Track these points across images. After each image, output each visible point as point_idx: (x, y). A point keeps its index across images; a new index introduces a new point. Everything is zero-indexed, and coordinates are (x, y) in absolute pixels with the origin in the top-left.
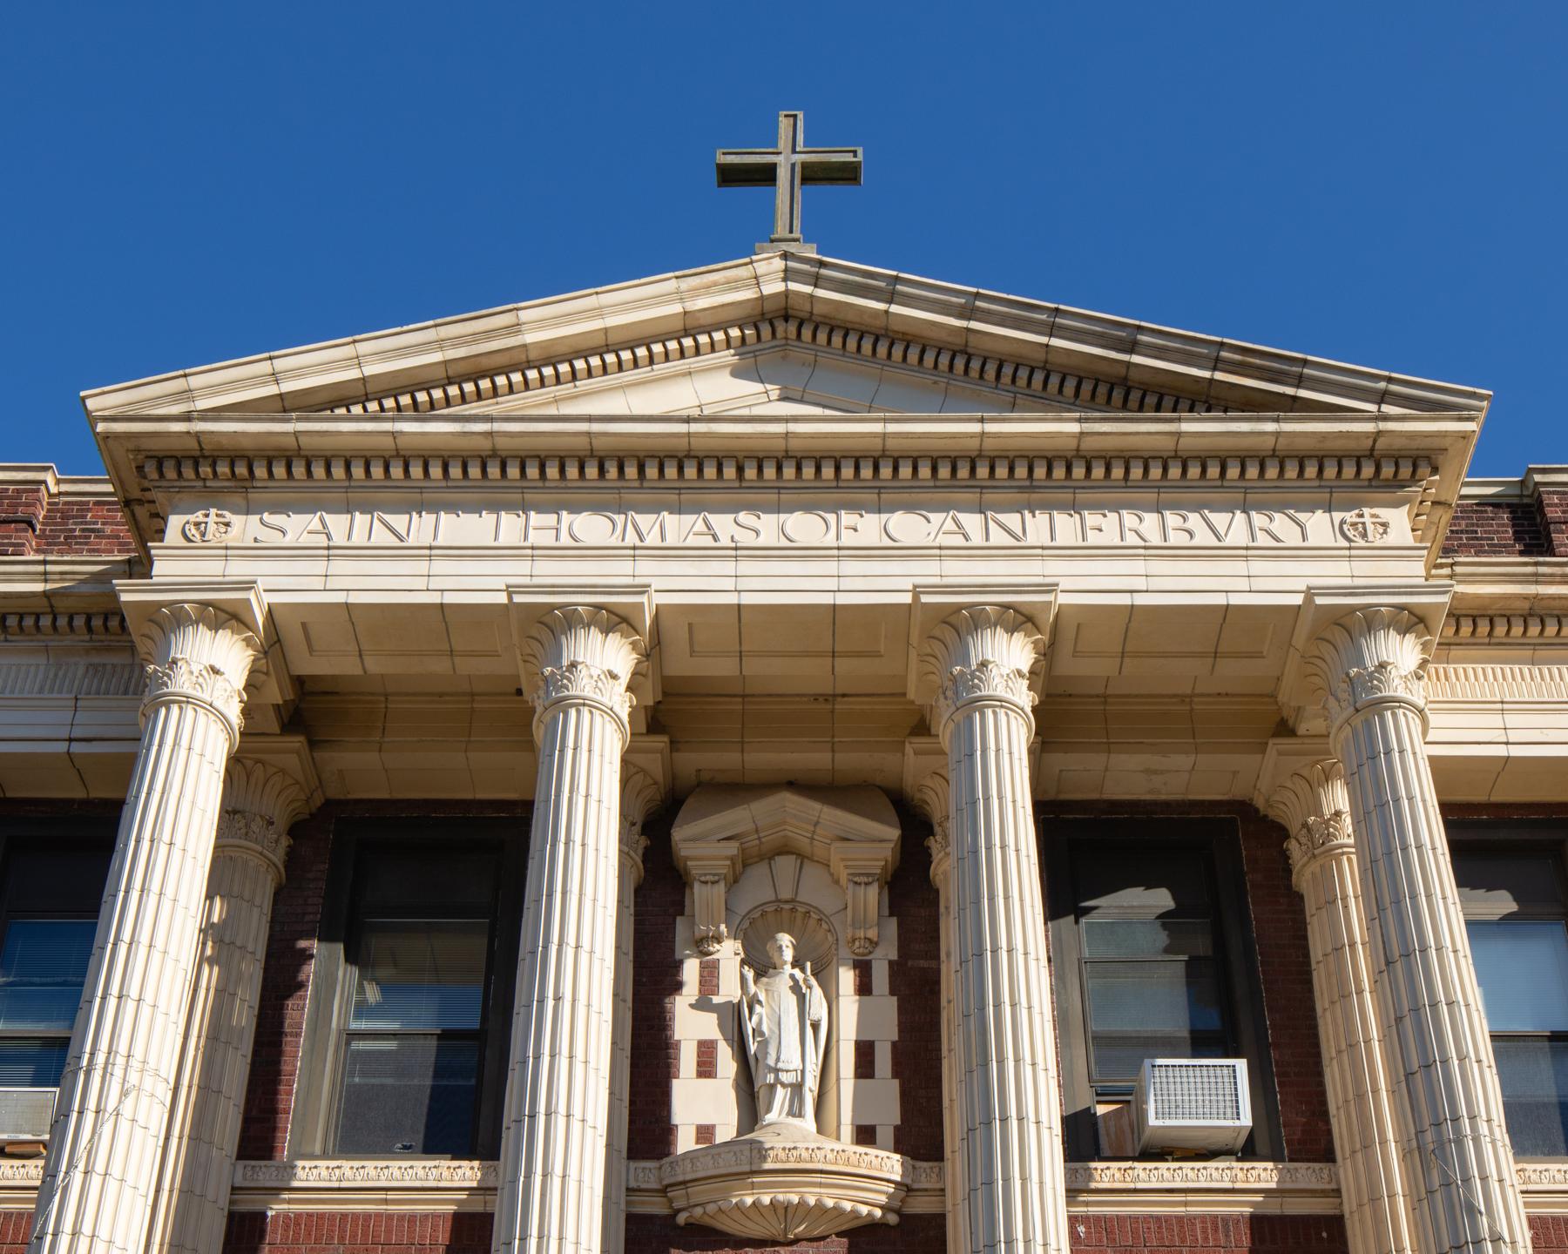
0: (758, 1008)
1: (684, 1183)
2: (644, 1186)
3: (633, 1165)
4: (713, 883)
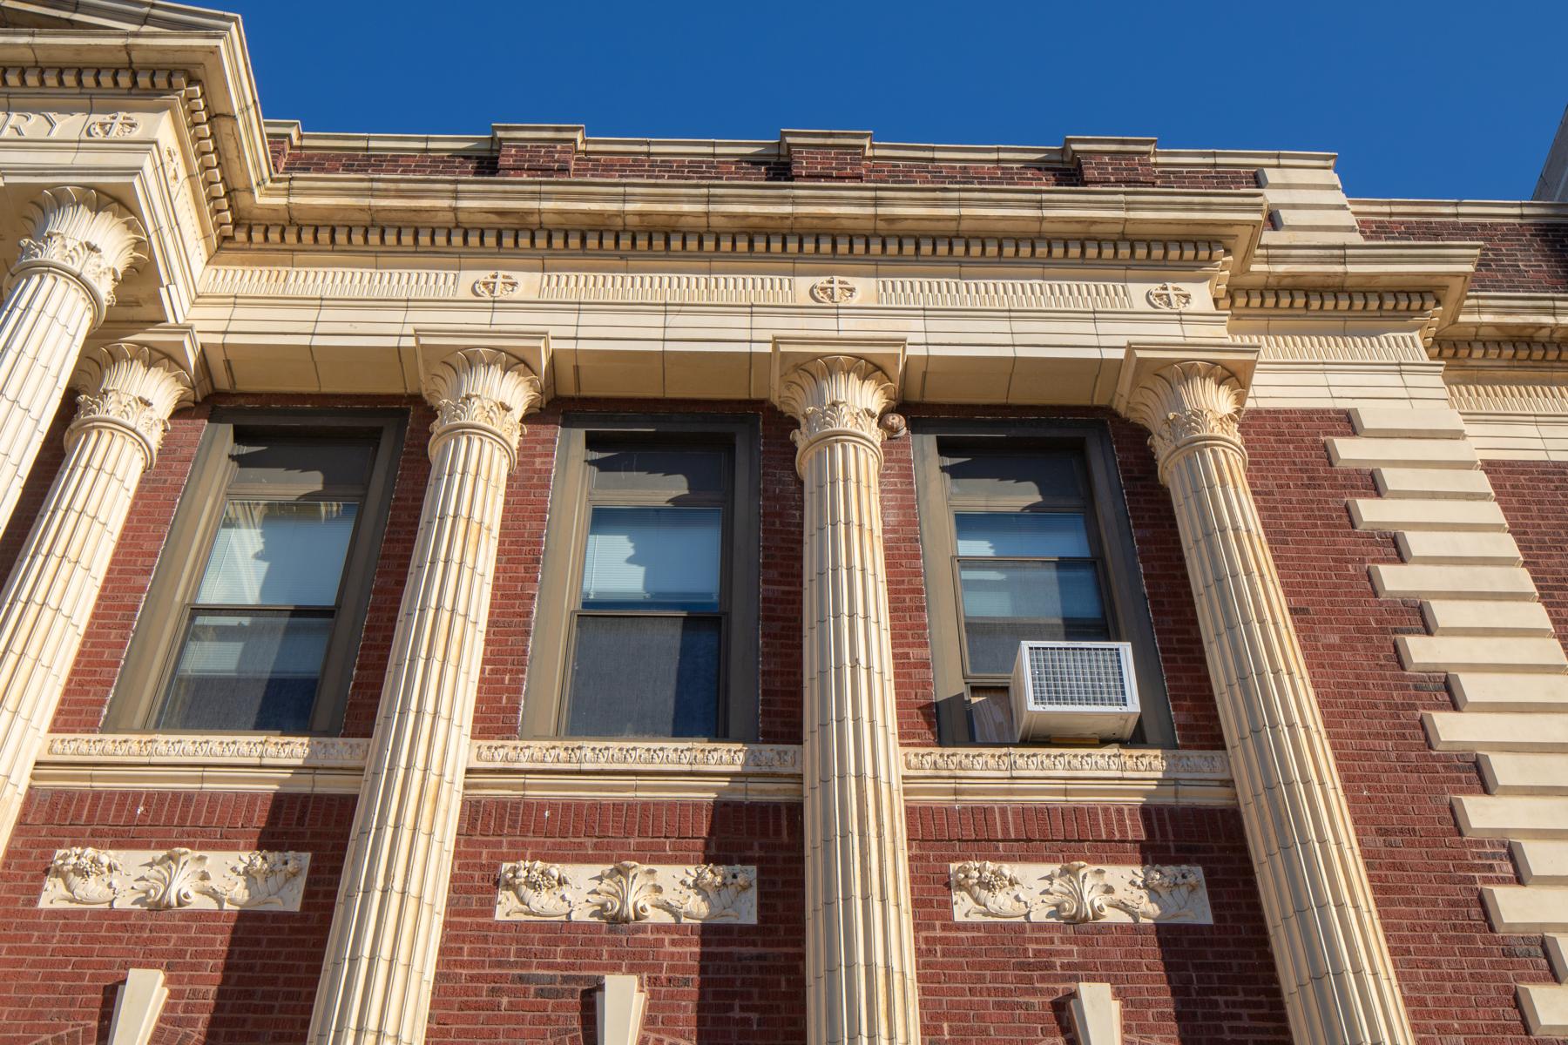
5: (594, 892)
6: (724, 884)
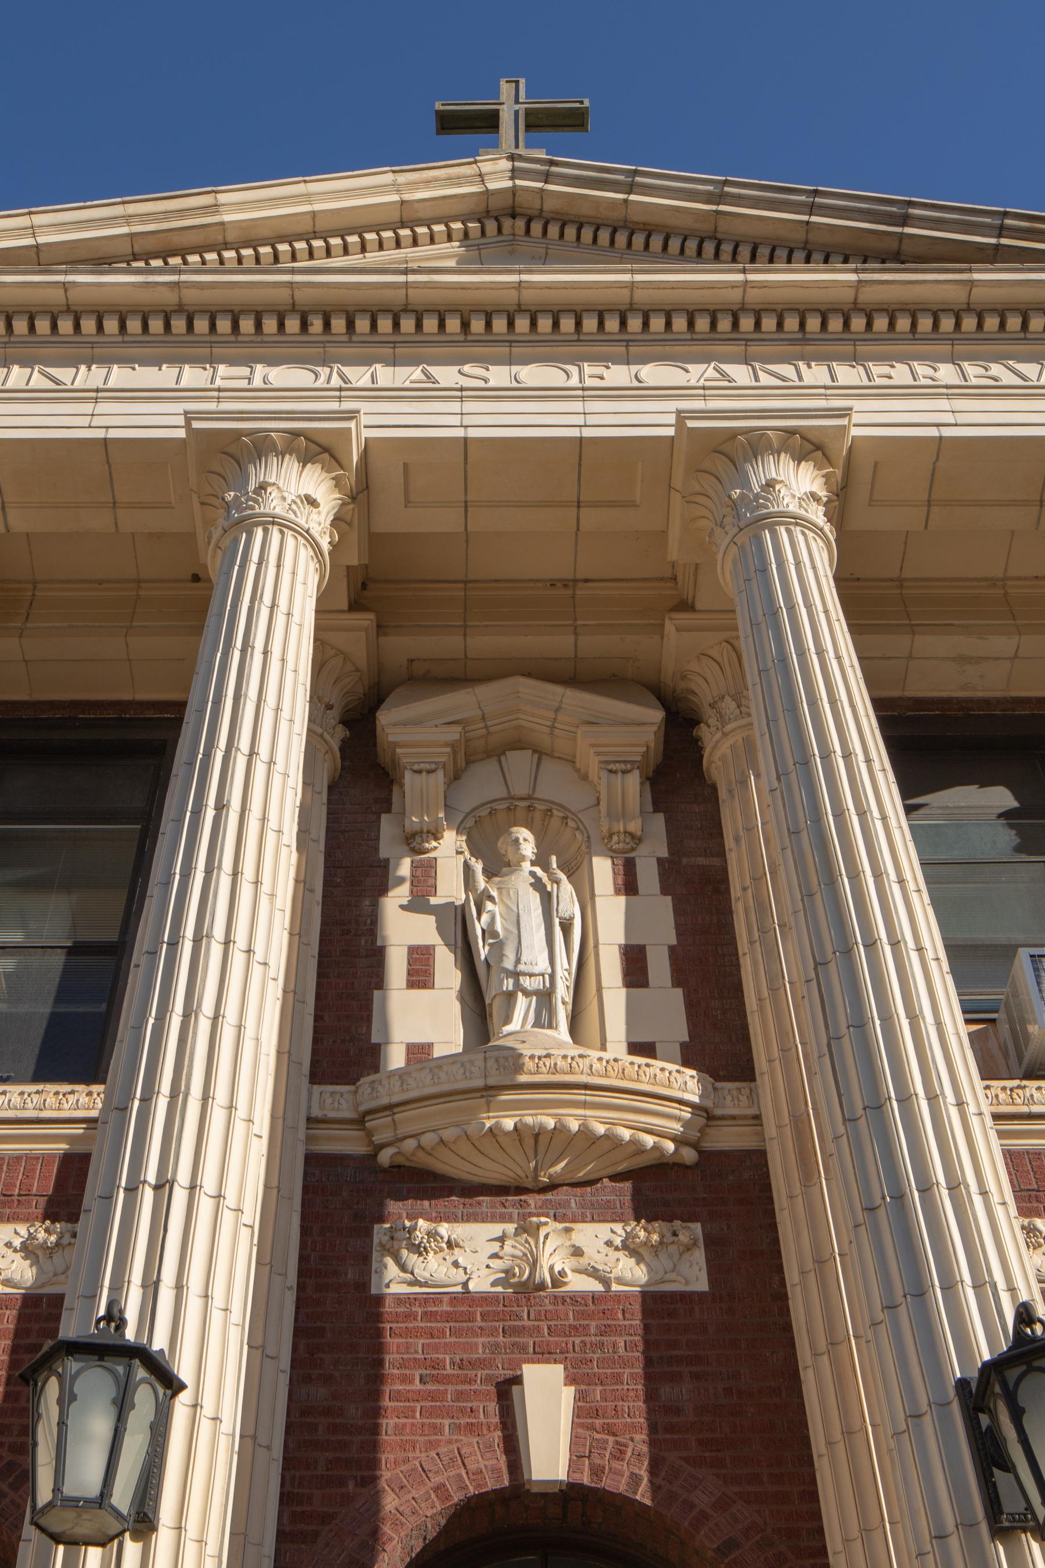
0: (489, 906)
1: (390, 1107)
2: (332, 1114)
3: (317, 1089)
4: (429, 772)
5: (495, 1256)
6: (661, 1243)
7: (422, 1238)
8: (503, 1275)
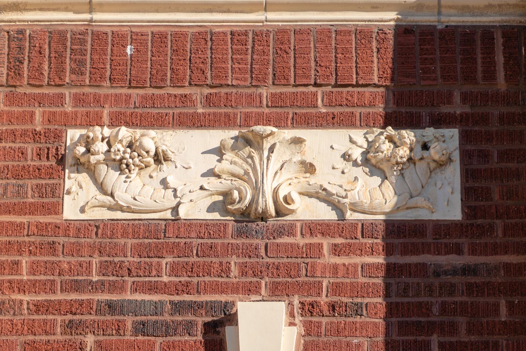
5: (211, 173)
7: (124, 152)
8: (221, 198)
